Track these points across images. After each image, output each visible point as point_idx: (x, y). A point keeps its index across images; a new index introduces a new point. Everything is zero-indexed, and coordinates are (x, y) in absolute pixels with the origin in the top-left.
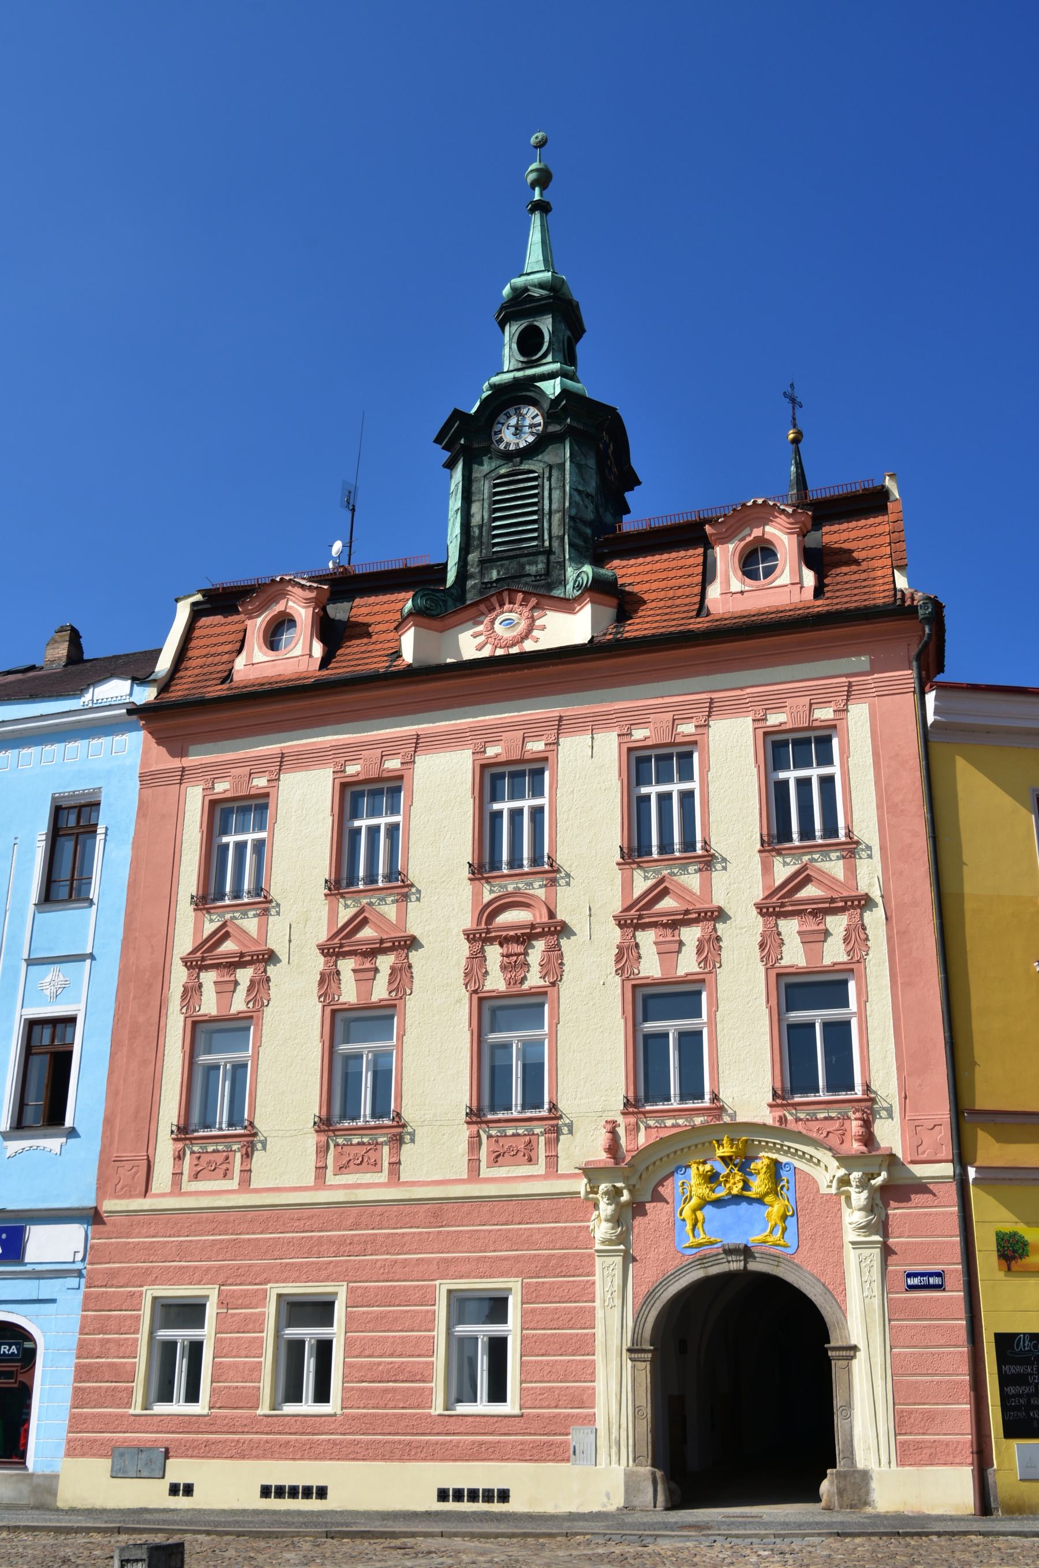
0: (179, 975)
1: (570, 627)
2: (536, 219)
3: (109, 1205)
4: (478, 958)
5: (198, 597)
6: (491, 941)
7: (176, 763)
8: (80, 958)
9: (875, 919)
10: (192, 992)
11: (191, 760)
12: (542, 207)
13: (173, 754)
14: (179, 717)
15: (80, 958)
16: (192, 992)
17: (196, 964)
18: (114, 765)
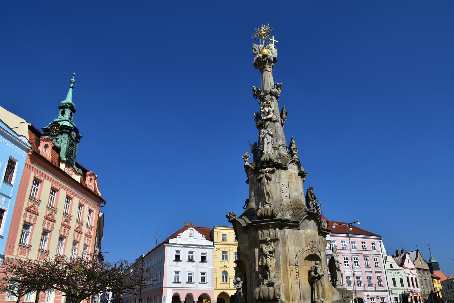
0: (24, 211)
1: (78, 178)
2: (71, 89)
3: (7, 256)
4: (61, 228)
5: (30, 125)
6: (63, 226)
7: (31, 165)
8: (9, 198)
9: (92, 239)
10: (25, 216)
11: (33, 166)
12: (73, 88)
13: (32, 163)
14: (36, 157)
15: (9, 198)
16: (25, 216)
17: (28, 210)
18: (22, 158)
